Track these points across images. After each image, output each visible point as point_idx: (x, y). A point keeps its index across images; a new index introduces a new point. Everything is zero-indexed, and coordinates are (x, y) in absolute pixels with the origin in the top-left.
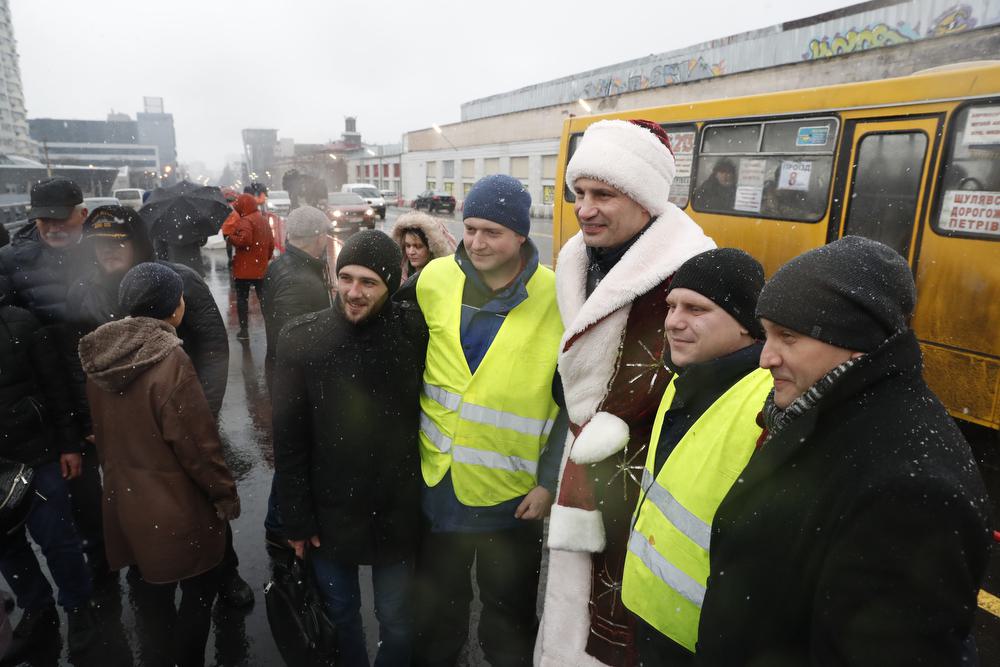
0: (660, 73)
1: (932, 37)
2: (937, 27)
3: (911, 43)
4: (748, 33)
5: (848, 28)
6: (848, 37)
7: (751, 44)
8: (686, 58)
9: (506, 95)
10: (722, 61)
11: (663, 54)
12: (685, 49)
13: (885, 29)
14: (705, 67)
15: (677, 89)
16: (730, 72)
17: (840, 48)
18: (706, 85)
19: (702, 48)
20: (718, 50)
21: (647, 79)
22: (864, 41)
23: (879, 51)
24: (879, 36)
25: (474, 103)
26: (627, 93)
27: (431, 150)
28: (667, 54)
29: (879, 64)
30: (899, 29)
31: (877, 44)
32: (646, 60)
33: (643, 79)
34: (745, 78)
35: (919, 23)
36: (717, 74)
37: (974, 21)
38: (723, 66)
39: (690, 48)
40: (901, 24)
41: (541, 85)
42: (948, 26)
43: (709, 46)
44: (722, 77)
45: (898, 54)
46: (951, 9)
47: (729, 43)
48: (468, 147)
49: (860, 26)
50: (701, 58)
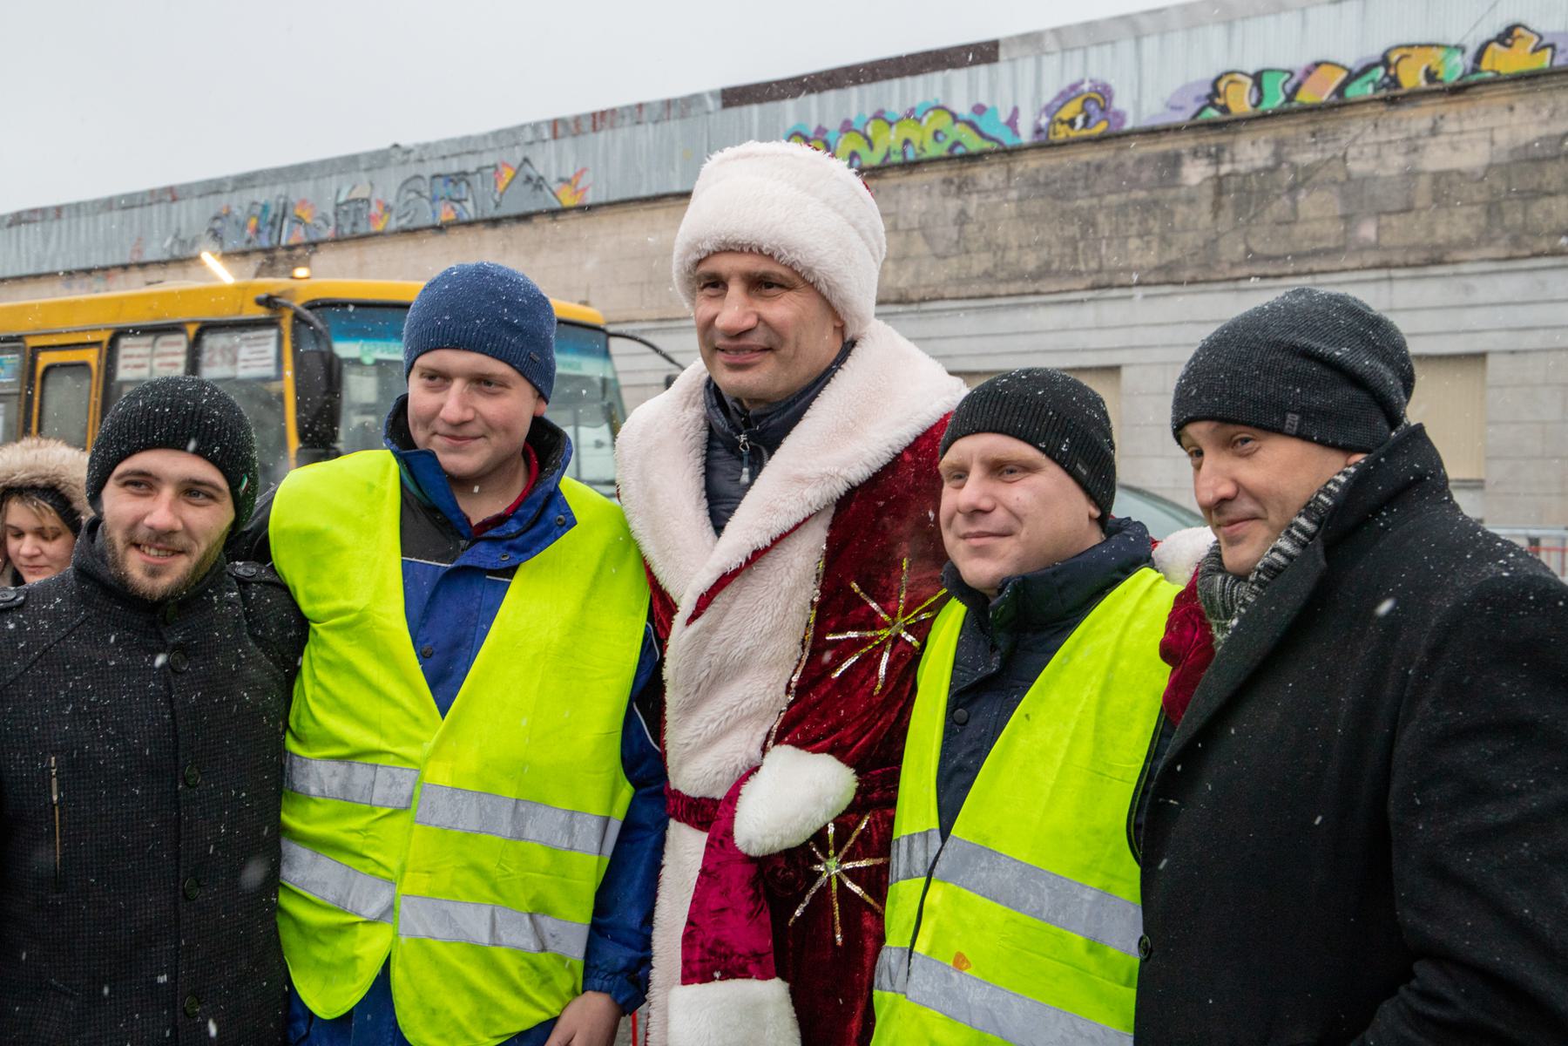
0: (419, 193)
1: (1044, 144)
3: (1010, 153)
4: (640, 106)
5: (868, 114)
6: (870, 132)
7: (647, 135)
8: (489, 159)
10: (579, 174)
11: (426, 146)
12: (485, 138)
13: (947, 119)
14: (538, 184)
16: (603, 199)
20: (567, 143)
21: (388, 209)
22: (907, 142)
23: (944, 166)
24: (936, 133)
26: (338, 240)
28: (437, 145)
29: (945, 195)
30: (976, 119)
31: (933, 150)
32: (379, 160)
33: (375, 209)
38: (580, 186)
39: (496, 135)
40: (979, 109)
41: (77, 208)
43: (547, 134)
44: (586, 209)
45: (985, 175)
47: (595, 129)
49: (895, 109)
50: (526, 160)
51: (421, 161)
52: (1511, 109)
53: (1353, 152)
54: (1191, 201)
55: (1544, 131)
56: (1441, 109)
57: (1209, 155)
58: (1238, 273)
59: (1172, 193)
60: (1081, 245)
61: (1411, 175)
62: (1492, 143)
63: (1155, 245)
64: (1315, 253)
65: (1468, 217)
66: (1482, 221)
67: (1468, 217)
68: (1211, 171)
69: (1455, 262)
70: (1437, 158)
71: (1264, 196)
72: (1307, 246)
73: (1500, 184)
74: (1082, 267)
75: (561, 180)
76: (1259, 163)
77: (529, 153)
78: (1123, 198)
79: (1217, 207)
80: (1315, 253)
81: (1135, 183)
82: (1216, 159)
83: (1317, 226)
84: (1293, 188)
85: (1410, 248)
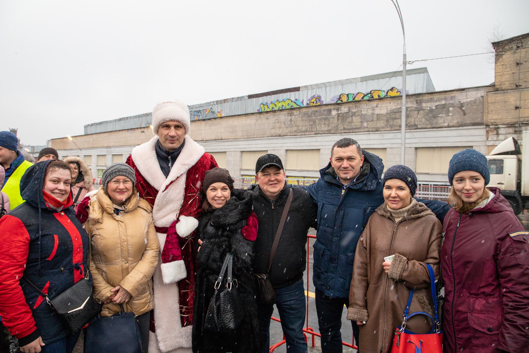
1: (308, 107)
2: (310, 102)
3: (300, 108)
4: (233, 98)
5: (276, 100)
6: (276, 104)
7: (234, 103)
8: (205, 108)
9: (111, 122)
11: (193, 106)
14: (213, 113)
15: (199, 123)
17: (273, 108)
18: (214, 121)
19: (212, 104)
20: (219, 105)
22: (283, 106)
23: (288, 110)
24: (288, 104)
25: (92, 125)
27: (66, 150)
28: (195, 105)
29: (288, 116)
30: (296, 101)
31: (288, 107)
34: (231, 119)
35: (303, 100)
36: (219, 116)
37: (322, 101)
39: (206, 103)
40: (296, 100)
42: (313, 103)
43: (215, 103)
45: (295, 112)
46: (314, 96)
47: (224, 102)
48: (88, 148)
49: (281, 100)
50: (211, 108)
51: (192, 108)
52: (390, 103)
53: (362, 110)
54: (333, 118)
55: (396, 107)
56: (378, 102)
57: (337, 110)
58: (342, 132)
59: (330, 116)
60: (313, 126)
61: (373, 114)
62: (387, 109)
63: (327, 126)
64: (356, 129)
65: (383, 123)
66: (386, 123)
67: (383, 123)
68: (337, 112)
69: (381, 131)
70: (377, 111)
71: (347, 118)
72: (354, 127)
73: (389, 117)
74: (313, 130)
75: (218, 112)
76: (346, 111)
77: (212, 107)
78: (321, 117)
79: (338, 120)
80: (356, 129)
81: (323, 114)
82: (338, 110)
83: (356, 123)
84: (352, 116)
85: (373, 128)
